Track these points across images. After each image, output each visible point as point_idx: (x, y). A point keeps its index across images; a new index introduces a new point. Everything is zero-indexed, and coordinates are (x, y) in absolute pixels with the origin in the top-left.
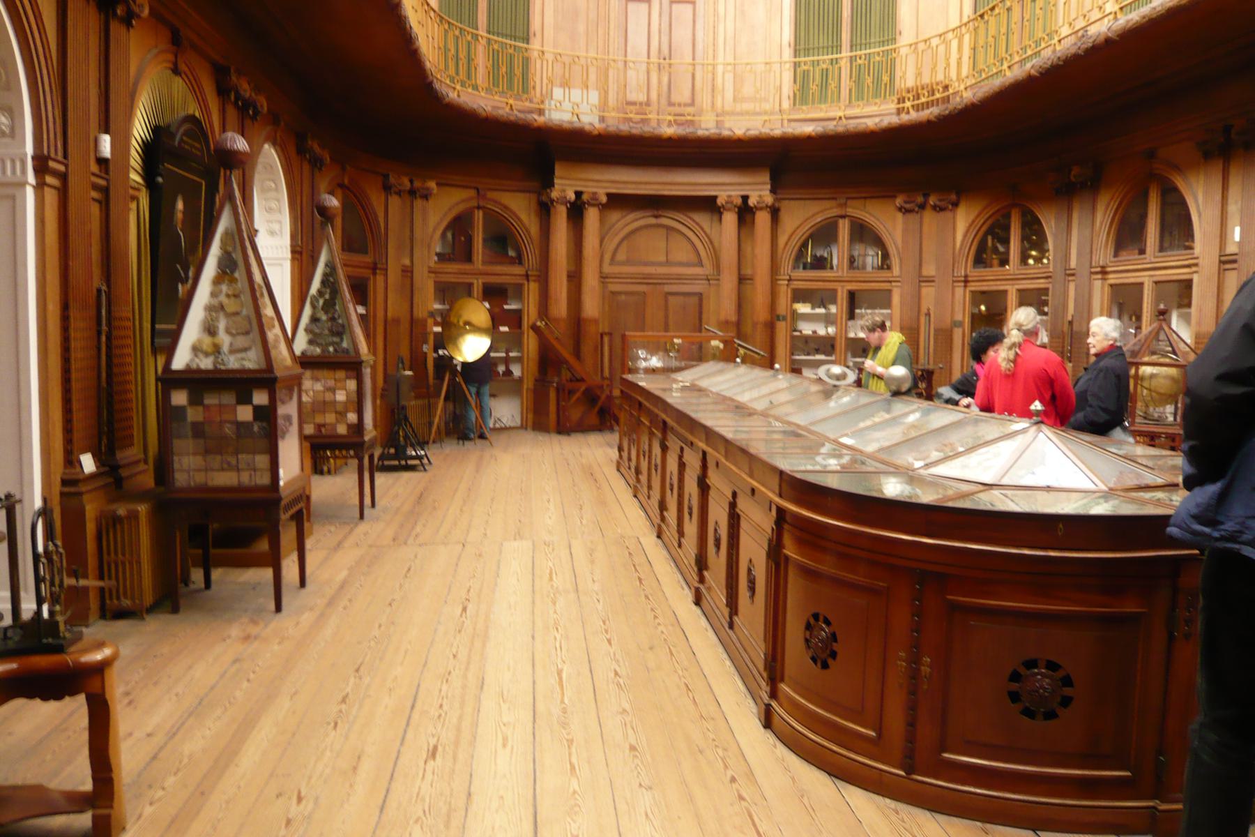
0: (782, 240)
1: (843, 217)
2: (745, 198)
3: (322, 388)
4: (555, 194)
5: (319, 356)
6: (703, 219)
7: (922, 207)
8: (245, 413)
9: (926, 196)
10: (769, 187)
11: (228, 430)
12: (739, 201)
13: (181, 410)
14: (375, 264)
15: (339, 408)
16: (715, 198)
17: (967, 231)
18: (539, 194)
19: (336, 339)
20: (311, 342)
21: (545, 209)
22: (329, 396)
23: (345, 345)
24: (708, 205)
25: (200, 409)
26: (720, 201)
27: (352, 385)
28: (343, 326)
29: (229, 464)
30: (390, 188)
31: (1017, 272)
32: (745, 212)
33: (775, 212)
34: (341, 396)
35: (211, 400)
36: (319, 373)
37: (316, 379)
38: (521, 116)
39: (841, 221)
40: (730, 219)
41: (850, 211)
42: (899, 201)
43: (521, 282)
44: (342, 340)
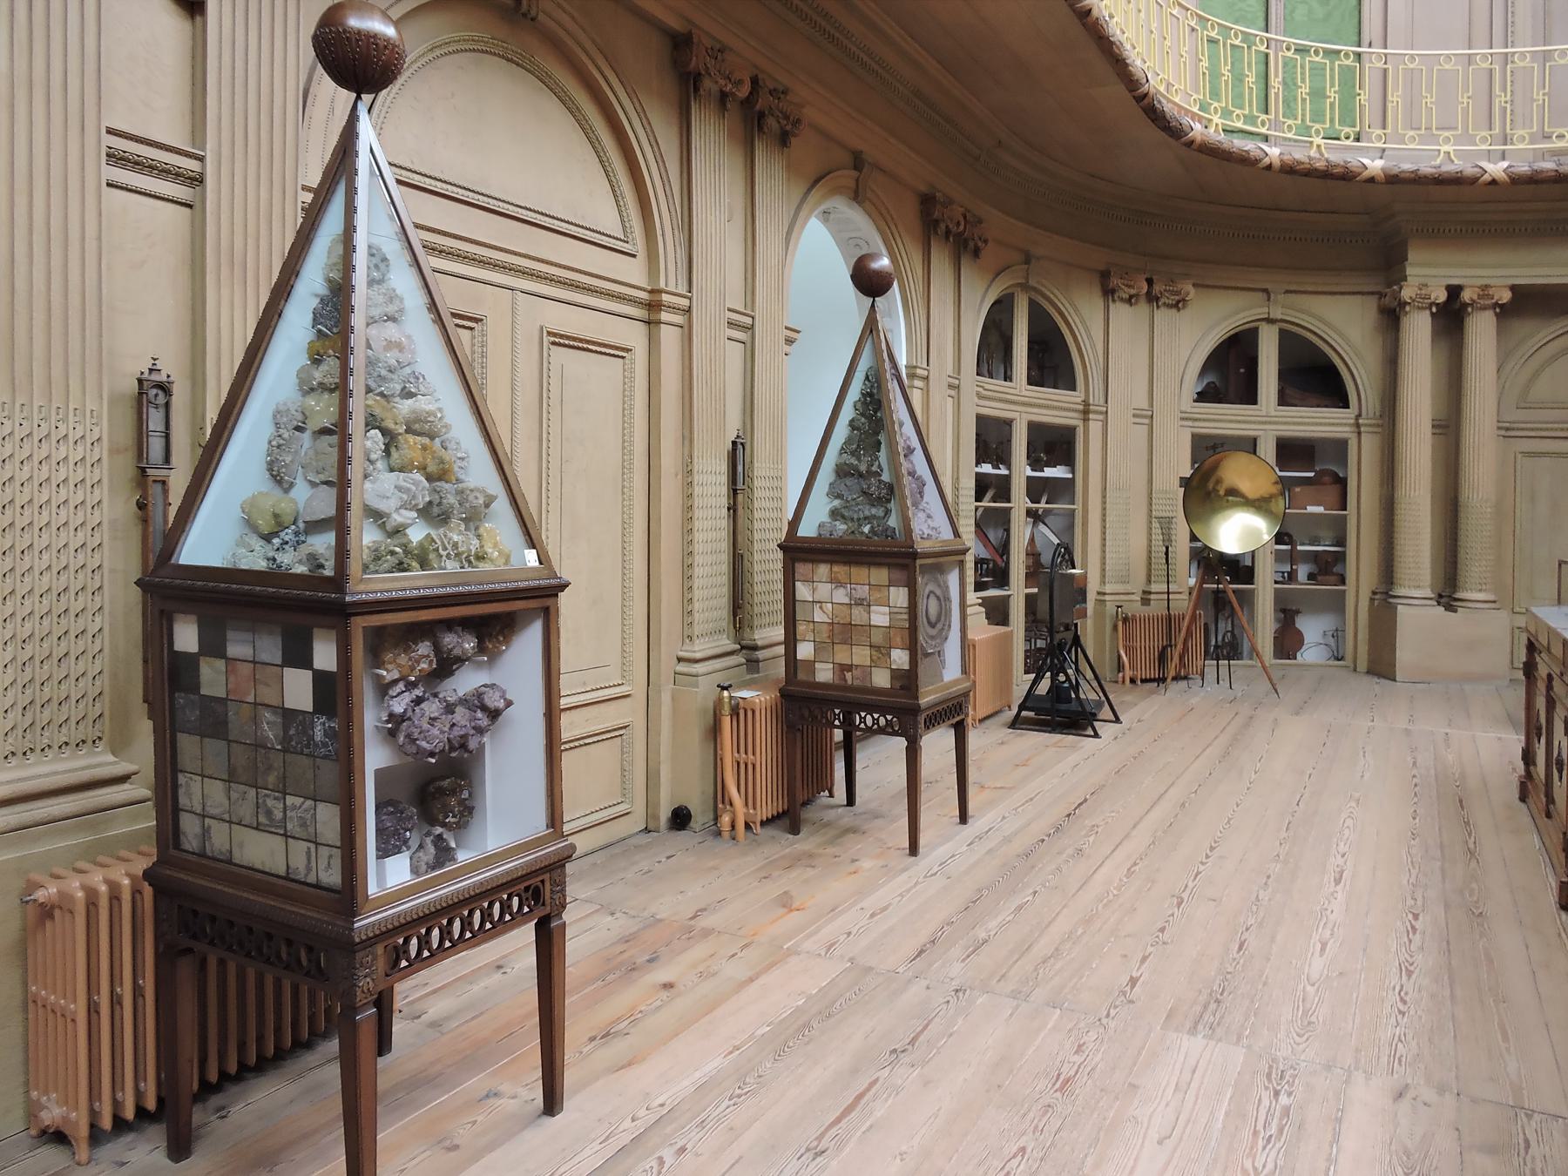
3: (847, 600)
5: (840, 541)
14: (1086, 403)
15: (877, 638)
18: (1381, 295)
19: (879, 512)
20: (835, 514)
21: (1391, 317)
22: (858, 615)
23: (893, 522)
27: (899, 596)
28: (891, 488)
29: (269, 813)
30: (1113, 292)
34: (880, 617)
36: (840, 570)
37: (836, 582)
44: (888, 512)
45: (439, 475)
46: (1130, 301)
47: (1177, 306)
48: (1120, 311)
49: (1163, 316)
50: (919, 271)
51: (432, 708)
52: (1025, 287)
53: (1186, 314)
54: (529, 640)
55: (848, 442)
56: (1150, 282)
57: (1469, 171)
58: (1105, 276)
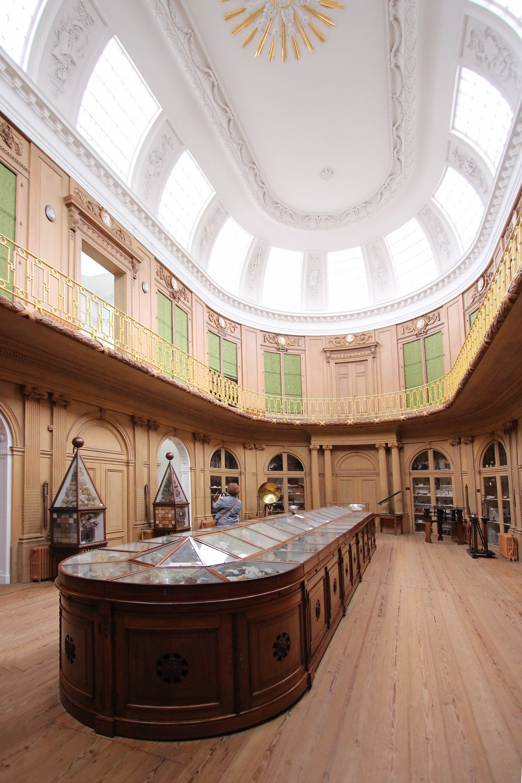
0: (406, 460)
1: (430, 449)
2: (387, 444)
4: (311, 447)
6: (373, 452)
7: (460, 443)
8: (71, 521)
9: (460, 439)
10: (396, 439)
11: (67, 526)
12: (384, 445)
13: (55, 519)
16: (375, 444)
17: (478, 451)
24: (372, 447)
25: (60, 519)
26: (376, 446)
31: (499, 469)
32: (388, 450)
33: (401, 449)
35: (63, 517)
38: (289, 421)
39: (429, 451)
40: (382, 453)
41: (432, 447)
42: (450, 441)
43: (237, 476)
45: (89, 495)
46: (250, 449)
47: (261, 450)
48: (248, 452)
49: (258, 452)
50: (193, 448)
51: (88, 523)
52: (223, 448)
53: (265, 452)
54: (102, 515)
55: (165, 486)
56: (255, 445)
57: (317, 423)
58: (244, 444)
